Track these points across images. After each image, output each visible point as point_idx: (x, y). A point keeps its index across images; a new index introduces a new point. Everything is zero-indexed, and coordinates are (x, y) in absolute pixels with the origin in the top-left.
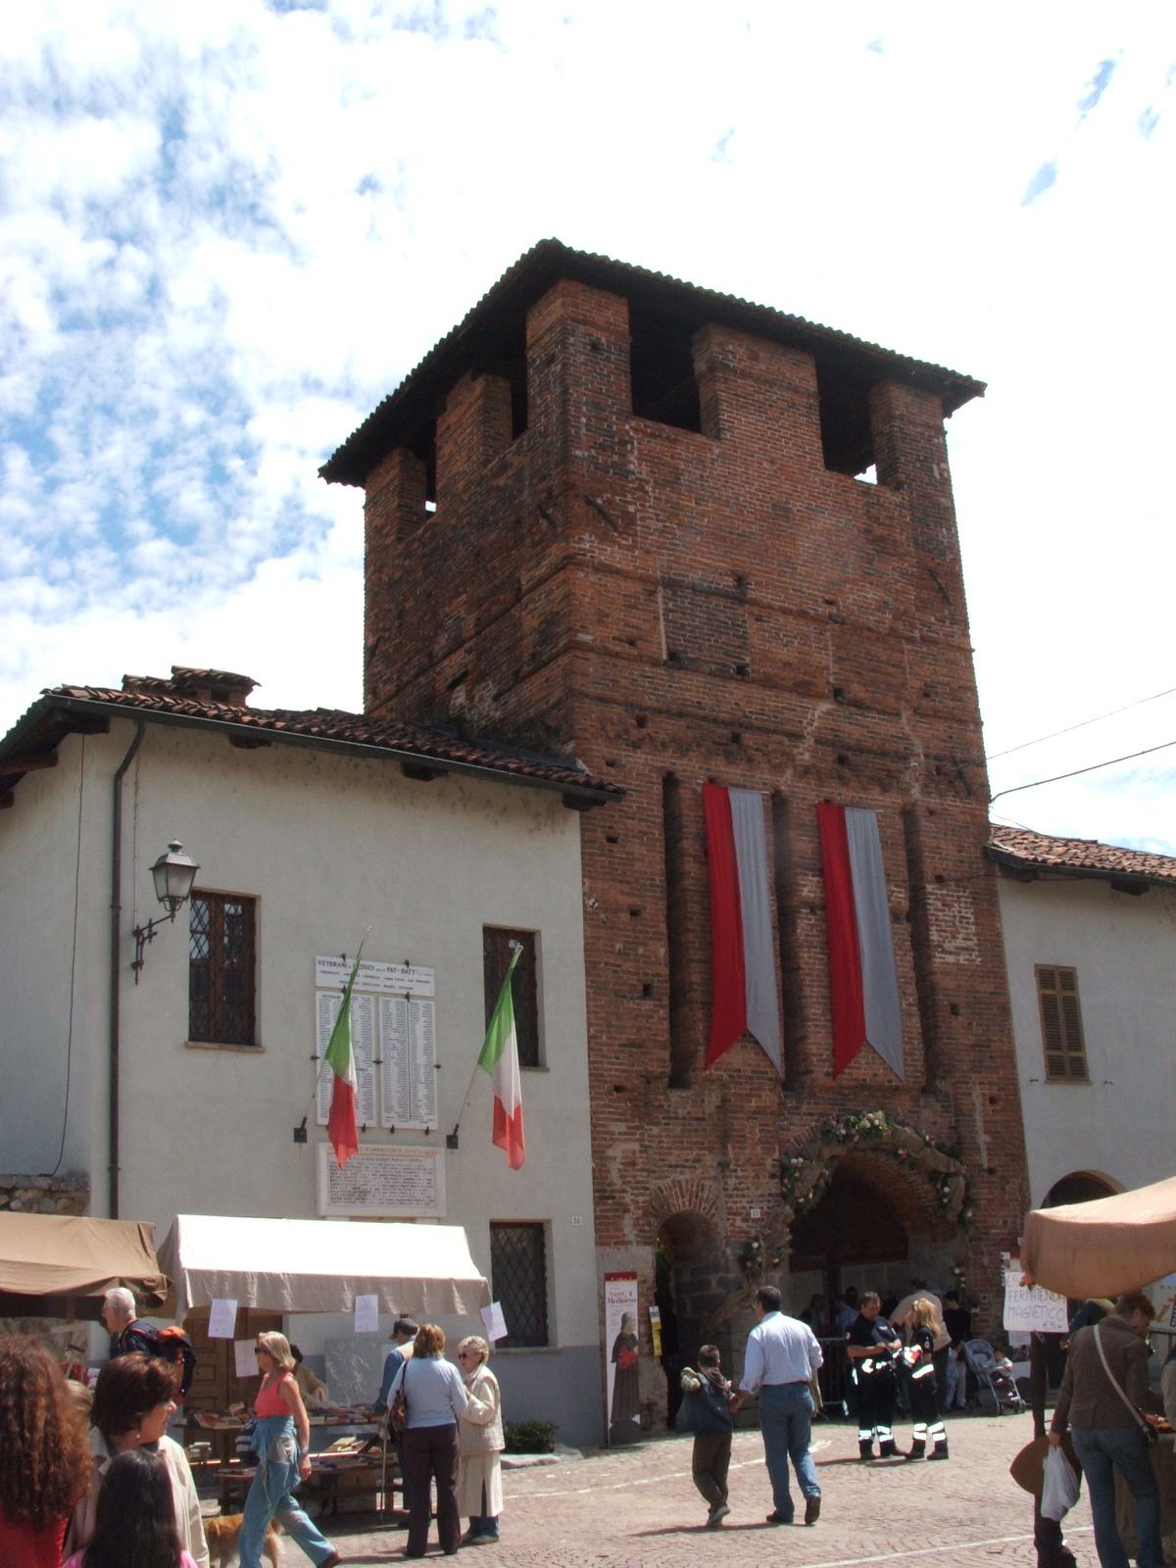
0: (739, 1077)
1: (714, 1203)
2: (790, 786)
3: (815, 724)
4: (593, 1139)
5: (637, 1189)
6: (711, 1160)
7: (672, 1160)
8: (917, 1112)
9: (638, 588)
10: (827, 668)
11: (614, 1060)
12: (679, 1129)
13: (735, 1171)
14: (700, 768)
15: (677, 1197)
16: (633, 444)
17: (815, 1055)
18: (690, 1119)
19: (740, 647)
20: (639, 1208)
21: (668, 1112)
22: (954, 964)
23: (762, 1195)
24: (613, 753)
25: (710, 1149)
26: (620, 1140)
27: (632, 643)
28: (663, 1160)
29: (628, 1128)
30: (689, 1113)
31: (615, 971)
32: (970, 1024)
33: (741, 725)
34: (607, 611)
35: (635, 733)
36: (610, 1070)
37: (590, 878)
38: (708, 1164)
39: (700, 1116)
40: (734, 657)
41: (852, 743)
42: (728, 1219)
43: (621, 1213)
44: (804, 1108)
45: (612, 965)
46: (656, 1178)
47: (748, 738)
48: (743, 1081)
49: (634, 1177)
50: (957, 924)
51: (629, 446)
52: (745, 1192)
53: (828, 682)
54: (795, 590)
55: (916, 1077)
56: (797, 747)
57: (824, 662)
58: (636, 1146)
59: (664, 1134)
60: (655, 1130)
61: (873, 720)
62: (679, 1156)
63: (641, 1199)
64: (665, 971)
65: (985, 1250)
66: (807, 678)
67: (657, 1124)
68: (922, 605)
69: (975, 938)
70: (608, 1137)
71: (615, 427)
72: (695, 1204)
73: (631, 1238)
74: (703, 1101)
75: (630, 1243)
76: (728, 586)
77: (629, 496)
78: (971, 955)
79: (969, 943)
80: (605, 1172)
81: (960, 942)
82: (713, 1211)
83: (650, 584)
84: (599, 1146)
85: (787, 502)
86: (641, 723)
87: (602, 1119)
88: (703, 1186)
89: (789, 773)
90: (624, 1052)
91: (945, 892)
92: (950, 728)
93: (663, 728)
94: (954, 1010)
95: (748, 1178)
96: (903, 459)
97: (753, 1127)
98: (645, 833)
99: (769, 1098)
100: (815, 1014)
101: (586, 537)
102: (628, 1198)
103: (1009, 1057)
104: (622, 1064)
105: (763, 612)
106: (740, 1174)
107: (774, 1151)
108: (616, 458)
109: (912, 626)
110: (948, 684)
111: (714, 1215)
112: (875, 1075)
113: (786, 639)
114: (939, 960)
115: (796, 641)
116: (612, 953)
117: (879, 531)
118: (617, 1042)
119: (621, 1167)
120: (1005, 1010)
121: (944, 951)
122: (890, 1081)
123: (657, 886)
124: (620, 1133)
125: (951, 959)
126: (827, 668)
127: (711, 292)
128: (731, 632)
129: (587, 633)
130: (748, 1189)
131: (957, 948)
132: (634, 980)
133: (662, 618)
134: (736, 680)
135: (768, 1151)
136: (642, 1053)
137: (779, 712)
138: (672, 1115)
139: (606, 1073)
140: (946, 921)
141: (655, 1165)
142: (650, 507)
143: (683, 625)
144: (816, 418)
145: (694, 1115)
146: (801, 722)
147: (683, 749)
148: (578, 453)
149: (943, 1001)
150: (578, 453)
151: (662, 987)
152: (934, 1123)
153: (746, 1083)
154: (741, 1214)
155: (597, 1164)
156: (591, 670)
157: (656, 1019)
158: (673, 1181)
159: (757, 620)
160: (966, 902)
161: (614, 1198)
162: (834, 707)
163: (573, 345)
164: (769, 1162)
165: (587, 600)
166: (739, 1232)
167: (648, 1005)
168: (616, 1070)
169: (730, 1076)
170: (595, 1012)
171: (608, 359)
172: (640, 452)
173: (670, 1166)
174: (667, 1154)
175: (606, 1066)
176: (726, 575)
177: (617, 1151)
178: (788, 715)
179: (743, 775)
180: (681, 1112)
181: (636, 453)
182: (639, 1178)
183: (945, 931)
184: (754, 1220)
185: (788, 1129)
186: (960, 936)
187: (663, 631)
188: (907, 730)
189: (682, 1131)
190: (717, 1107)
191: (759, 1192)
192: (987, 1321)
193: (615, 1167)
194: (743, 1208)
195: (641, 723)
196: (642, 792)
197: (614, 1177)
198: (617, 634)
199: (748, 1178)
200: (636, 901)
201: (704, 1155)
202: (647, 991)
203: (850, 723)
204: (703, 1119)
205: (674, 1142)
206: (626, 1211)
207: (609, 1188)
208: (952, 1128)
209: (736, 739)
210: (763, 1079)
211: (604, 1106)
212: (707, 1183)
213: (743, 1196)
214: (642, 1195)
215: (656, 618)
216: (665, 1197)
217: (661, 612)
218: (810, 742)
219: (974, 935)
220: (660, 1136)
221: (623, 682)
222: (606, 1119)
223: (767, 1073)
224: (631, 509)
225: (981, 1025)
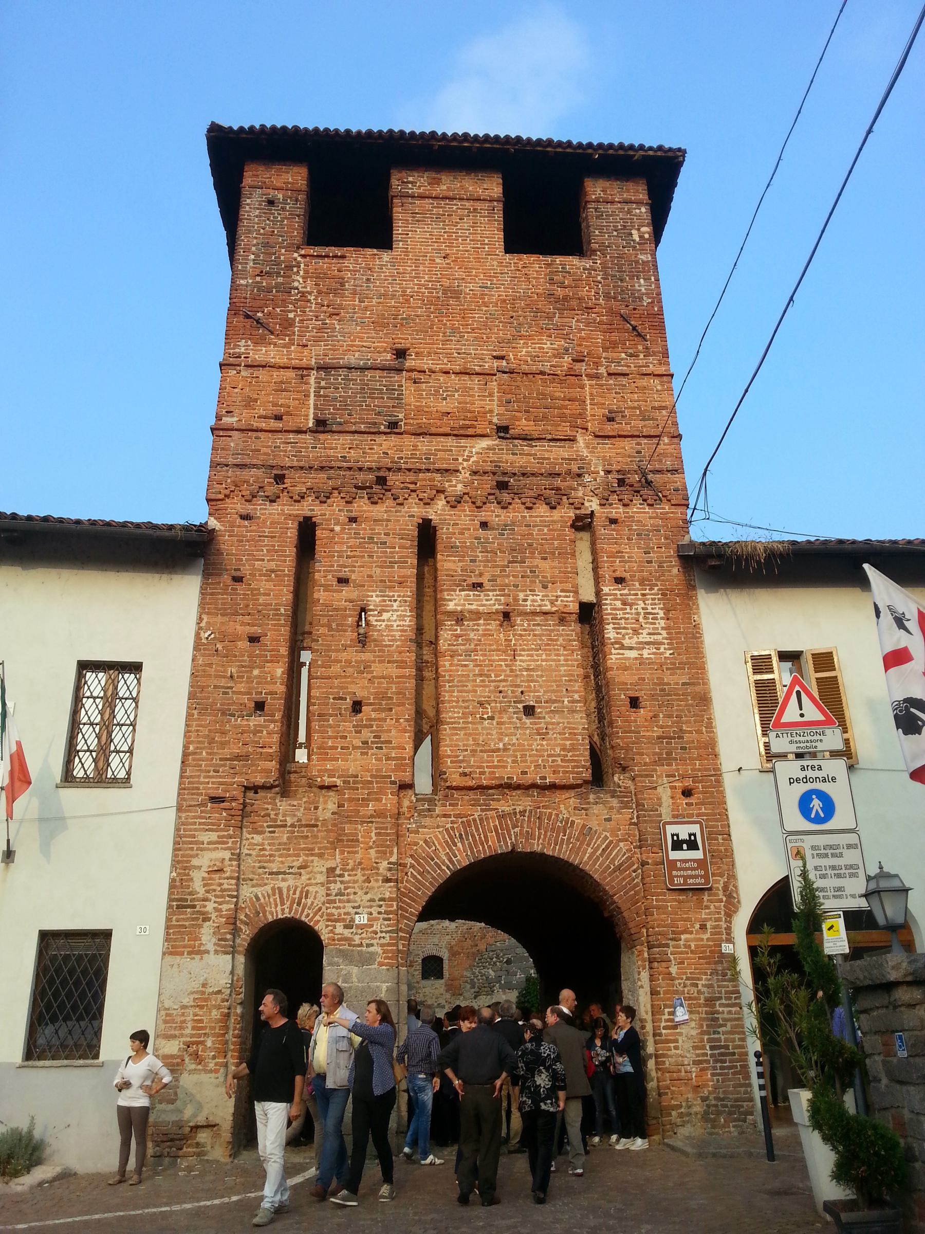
0: (355, 782)
1: (320, 909)
2: (441, 515)
3: (472, 459)
4: (175, 850)
5: (222, 896)
6: (319, 866)
7: (274, 867)
8: (586, 810)
9: (291, 374)
10: (491, 411)
11: (212, 773)
12: (286, 836)
13: (341, 876)
14: (339, 510)
15: (276, 906)
16: (300, 267)
17: (449, 756)
18: (301, 826)
19: (393, 407)
20: (221, 916)
21: (275, 820)
22: (636, 659)
23: (372, 900)
24: (249, 508)
25: (321, 856)
26: (208, 849)
27: (278, 418)
28: (264, 868)
29: (219, 837)
30: (299, 820)
31: (225, 693)
32: (656, 716)
33: (389, 469)
34: (256, 396)
35: (272, 490)
36: (208, 783)
37: (208, 614)
38: (316, 869)
39: (313, 822)
40: (386, 416)
41: (516, 470)
42: (327, 926)
43: (200, 922)
44: (438, 810)
45: (223, 687)
46: (253, 886)
47: (394, 479)
48: (359, 786)
49: (220, 885)
50: (641, 620)
51: (295, 269)
52: (352, 897)
53: (490, 422)
54: (459, 354)
55: (577, 773)
56: (450, 481)
57: (488, 408)
58: (227, 855)
59: (266, 842)
60: (258, 838)
61: (540, 449)
62: (282, 863)
63: (224, 907)
64: (281, 688)
65: (672, 957)
66: (467, 422)
67: (262, 833)
68: (612, 346)
69: (664, 633)
70: (195, 847)
71: (282, 258)
72: (297, 911)
73: (210, 947)
74: (316, 808)
75: (208, 952)
76: (386, 360)
77: (290, 306)
78: (658, 649)
79: (656, 637)
80: (187, 881)
81: (644, 637)
82: (317, 918)
83: (302, 370)
84: (183, 856)
85: (458, 286)
86: (279, 479)
87: (191, 830)
88: (307, 892)
89: (441, 503)
90: (224, 765)
91: (626, 592)
92: (638, 444)
93: (298, 483)
94: (634, 703)
95: (355, 882)
96: (597, 232)
97: (368, 832)
98: (273, 571)
99: (388, 800)
100: (450, 718)
101: (243, 343)
102: (210, 906)
103: (710, 749)
104: (220, 777)
105: (418, 376)
106: (347, 878)
107: (391, 853)
108: (280, 280)
109: (597, 365)
110: (639, 408)
111: (319, 921)
112: (525, 773)
113: (445, 394)
114: (614, 657)
115: (456, 394)
116: (224, 677)
117: (560, 292)
118: (218, 757)
119: (206, 875)
120: (704, 700)
121: (623, 647)
122: (544, 778)
123: (281, 615)
124: (209, 843)
125: (633, 654)
126: (491, 411)
127: (370, 133)
128: (385, 397)
129: (233, 416)
130: (355, 893)
131: (641, 643)
132: (245, 699)
133: (312, 395)
134: (385, 433)
135: (383, 854)
136: (244, 766)
137: (431, 454)
138: (279, 823)
139: (201, 787)
140: (628, 619)
141: (254, 873)
142: (310, 311)
143: (335, 399)
144: (499, 216)
145: (304, 823)
146: (457, 459)
147: (323, 497)
148: (243, 282)
149: (620, 698)
150: (243, 282)
151: (276, 705)
152: (609, 820)
153: (362, 788)
154: (344, 920)
155: (179, 874)
156: (232, 445)
157: (265, 732)
158: (273, 889)
159: (415, 382)
160: (653, 599)
161: (194, 907)
162: (496, 442)
163: (248, 204)
164: (384, 864)
165: (236, 390)
166: (339, 940)
167: (256, 720)
168: (213, 783)
169: (344, 782)
170: (198, 731)
171: (283, 209)
172: (306, 272)
173: (271, 873)
174: (270, 861)
175: (202, 780)
176: (385, 351)
177: (204, 861)
178: (440, 455)
179: (386, 512)
180: (289, 821)
181: (302, 273)
182: (226, 886)
183: (625, 628)
184: (358, 927)
185: (417, 832)
186: (645, 632)
187: (312, 406)
188: (585, 453)
189: (288, 838)
190: (333, 813)
191: (369, 896)
192: (676, 1041)
193: (198, 877)
194: (348, 914)
195: (279, 479)
196: (275, 537)
197: (198, 886)
198: (264, 413)
199: (355, 882)
200: (257, 630)
201: (312, 861)
202: (260, 706)
203: (513, 454)
204: (316, 826)
205: (279, 850)
206: (209, 919)
207: (189, 897)
208: (634, 824)
209: (381, 481)
210: (385, 783)
211: (195, 817)
212: (311, 889)
213: (349, 901)
214: (228, 902)
215: (307, 396)
216: (261, 905)
217: (312, 390)
218: (465, 475)
219: (663, 628)
220: (263, 844)
221: (264, 450)
222: (196, 830)
223: (390, 777)
224: (291, 315)
225: (670, 716)
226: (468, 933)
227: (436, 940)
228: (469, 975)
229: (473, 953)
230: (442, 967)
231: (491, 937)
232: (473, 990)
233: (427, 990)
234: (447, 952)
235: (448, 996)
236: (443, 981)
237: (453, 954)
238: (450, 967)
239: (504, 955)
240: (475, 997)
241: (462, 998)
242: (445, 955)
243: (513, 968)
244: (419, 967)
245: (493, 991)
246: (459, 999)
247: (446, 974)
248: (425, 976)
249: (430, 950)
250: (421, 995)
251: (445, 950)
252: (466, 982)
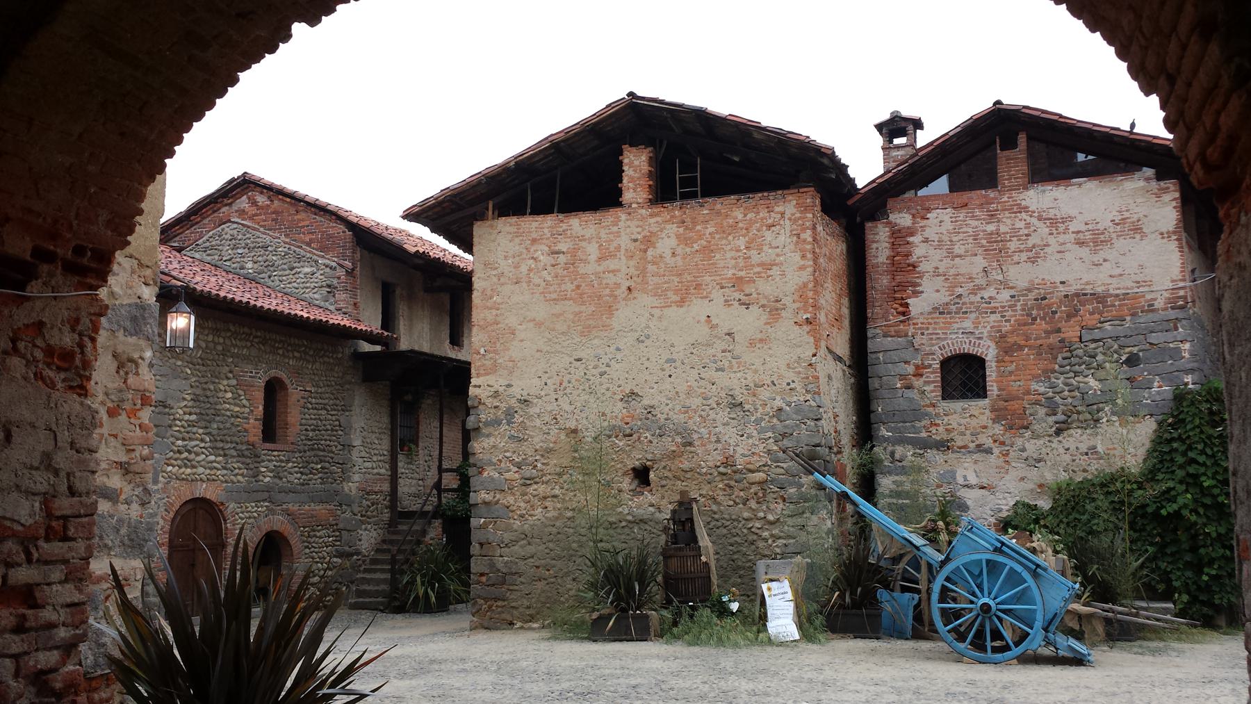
226: (1039, 308)
227: (968, 324)
228: (1042, 389)
229: (1051, 347)
230: (984, 376)
231: (1092, 314)
232: (1051, 419)
233: (954, 421)
234: (993, 345)
235: (998, 429)
236: (987, 401)
237: (1007, 349)
238: (1001, 375)
239: (1121, 347)
240: (1058, 432)
241: (1028, 434)
242: (990, 352)
243: (1141, 372)
244: (937, 377)
245: (1097, 421)
246: (1022, 436)
247: (993, 388)
248: (949, 392)
249: (957, 343)
250: (941, 429)
251: (989, 343)
252: (1037, 403)
